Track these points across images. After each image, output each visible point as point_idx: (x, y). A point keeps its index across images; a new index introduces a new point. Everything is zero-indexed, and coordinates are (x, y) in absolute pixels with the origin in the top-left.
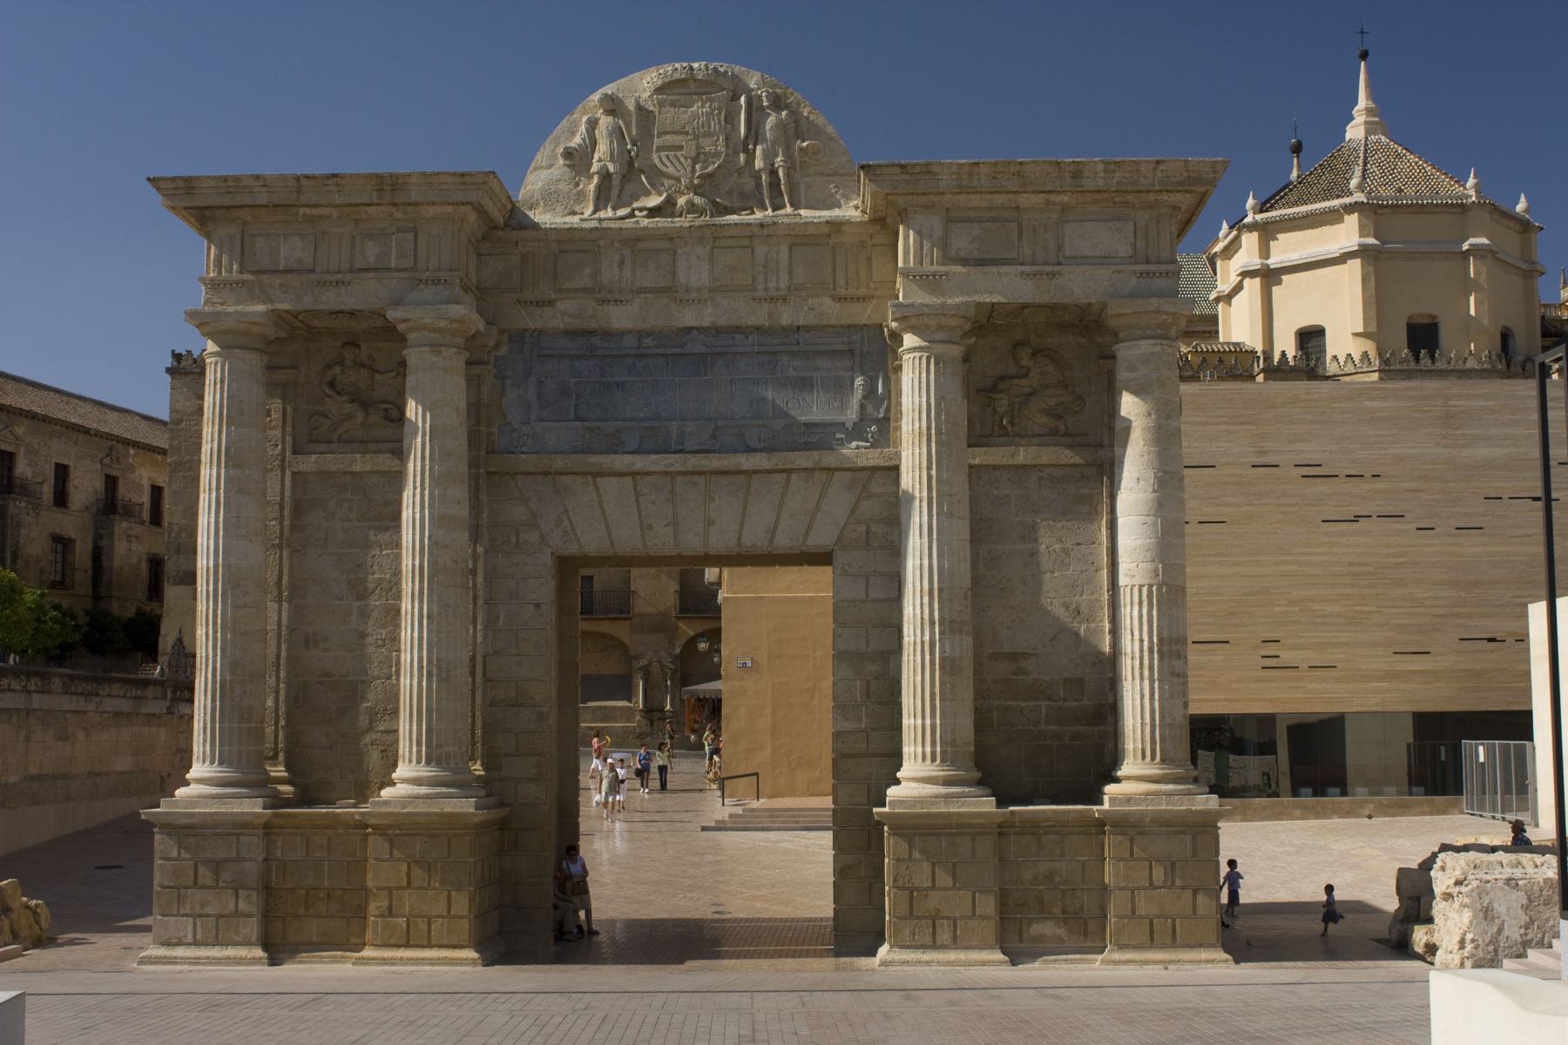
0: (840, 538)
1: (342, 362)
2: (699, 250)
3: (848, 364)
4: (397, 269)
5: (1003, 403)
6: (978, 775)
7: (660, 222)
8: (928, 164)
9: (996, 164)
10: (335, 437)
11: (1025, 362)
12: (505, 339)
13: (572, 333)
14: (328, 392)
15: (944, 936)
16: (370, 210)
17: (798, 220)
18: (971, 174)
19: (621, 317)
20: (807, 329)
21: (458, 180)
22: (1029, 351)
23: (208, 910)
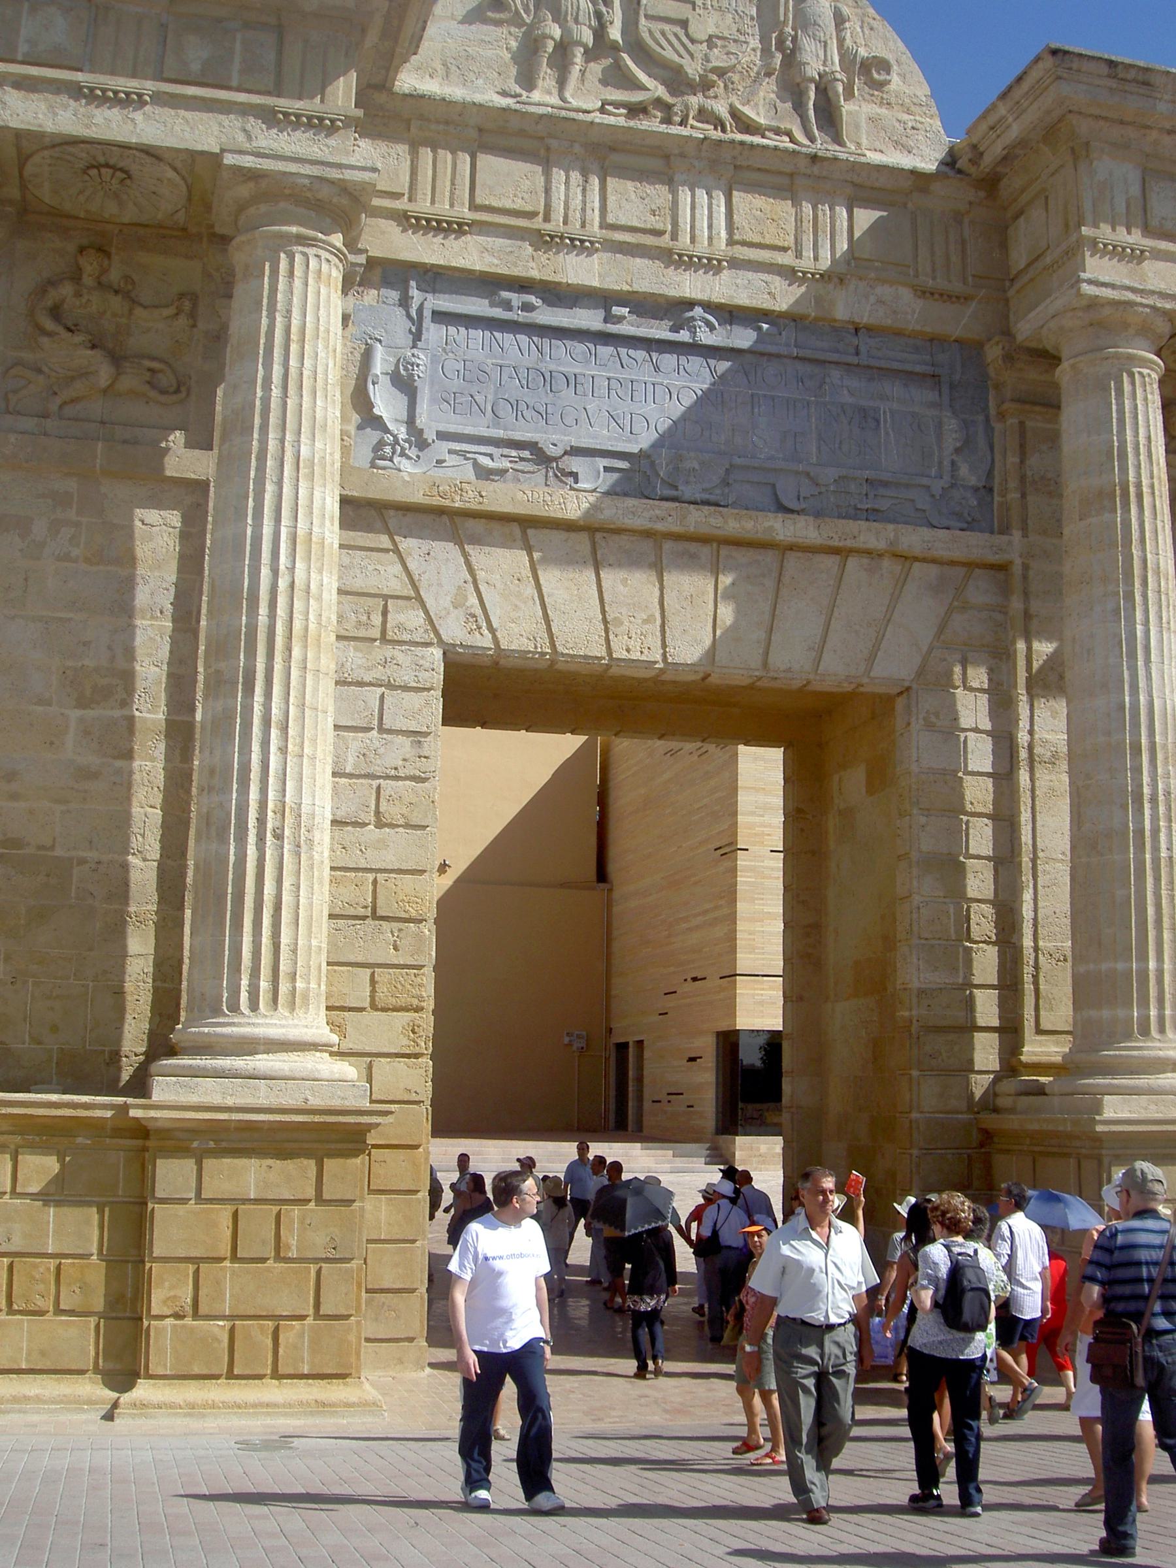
0: (920, 673)
1: (76, 277)
3: (931, 396)
8: (1147, 70)
10: (54, 408)
14: (49, 325)
17: (863, 160)
20: (870, 330)
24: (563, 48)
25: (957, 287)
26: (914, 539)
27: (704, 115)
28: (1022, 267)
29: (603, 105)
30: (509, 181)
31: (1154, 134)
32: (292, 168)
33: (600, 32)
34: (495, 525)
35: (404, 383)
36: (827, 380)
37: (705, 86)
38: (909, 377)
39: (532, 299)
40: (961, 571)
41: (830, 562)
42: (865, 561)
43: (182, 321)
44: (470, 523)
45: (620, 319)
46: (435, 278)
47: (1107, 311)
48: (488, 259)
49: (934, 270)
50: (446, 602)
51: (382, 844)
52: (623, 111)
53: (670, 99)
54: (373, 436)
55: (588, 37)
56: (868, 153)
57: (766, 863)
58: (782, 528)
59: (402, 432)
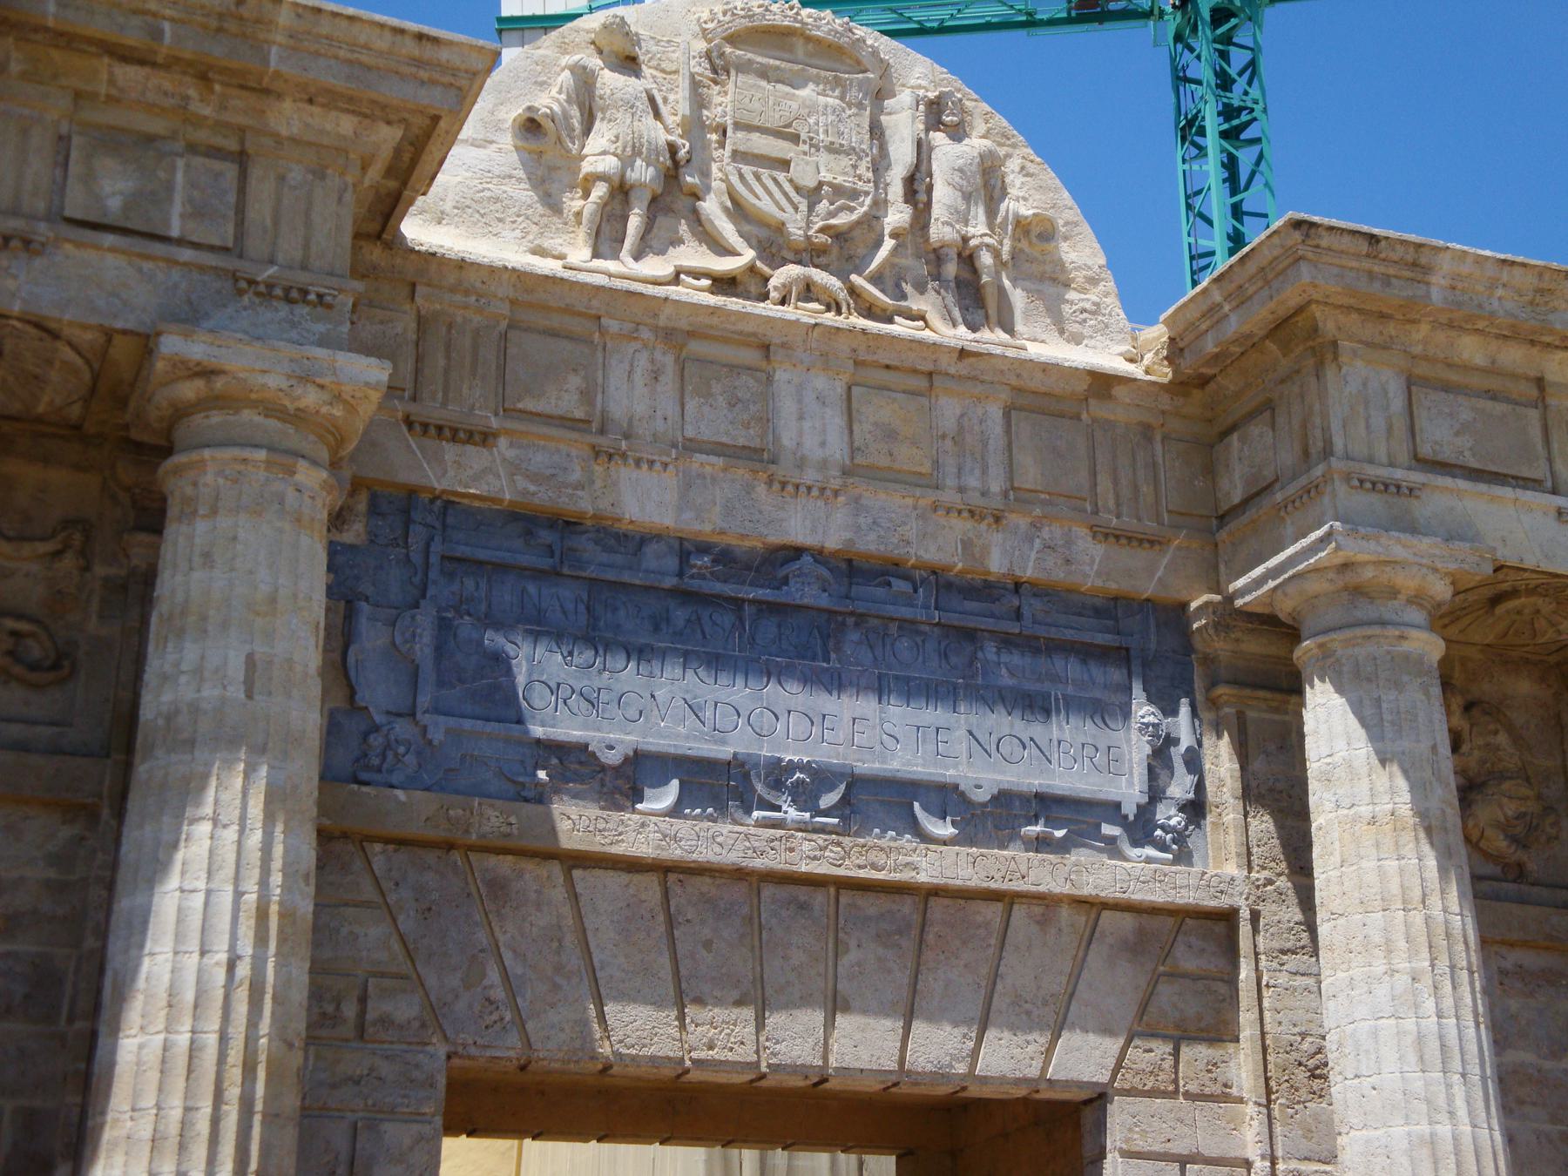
2: (820, 382)
4: (180, 242)
7: (734, 304)
12: (362, 506)
13: (525, 520)
17: (1023, 355)
25: (1150, 526)
28: (1236, 500)
29: (678, 274)
36: (980, 654)
40: (1170, 921)
43: (68, 562)
49: (1118, 505)
50: (454, 981)
52: (706, 282)
56: (1028, 344)
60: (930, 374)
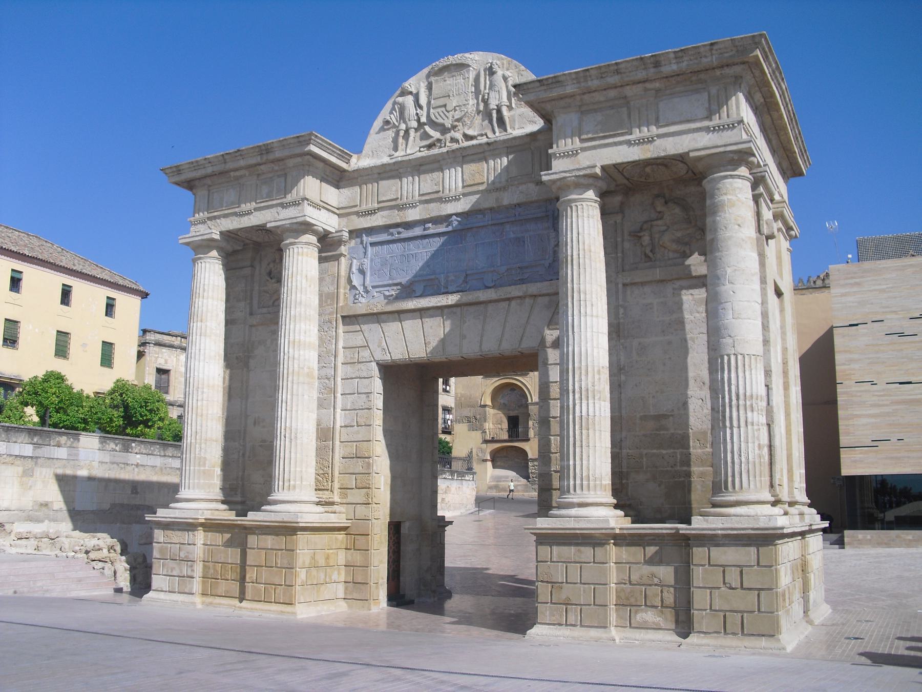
5: (646, 239)
6: (615, 501)
8: (555, 77)
9: (600, 68)
10: (271, 303)
11: (659, 209)
15: (571, 620)
16: (262, 167)
17: (511, 136)
18: (585, 77)
19: (413, 215)
20: (519, 205)
21: (296, 140)
22: (663, 201)
23: (175, 573)
24: (407, 132)
26: (533, 288)
27: (453, 140)
30: (389, 189)
31: (578, 98)
32: (284, 222)
33: (418, 120)
34: (390, 316)
35: (362, 272)
37: (454, 127)
38: (536, 219)
39: (400, 229)
41: (504, 304)
42: (519, 301)
44: (383, 316)
45: (429, 228)
46: (370, 231)
47: (558, 183)
48: (384, 220)
51: (358, 432)
53: (441, 138)
54: (354, 292)
55: (414, 124)
57: (854, 389)
58: (483, 295)
59: (361, 289)
60: (483, 152)
